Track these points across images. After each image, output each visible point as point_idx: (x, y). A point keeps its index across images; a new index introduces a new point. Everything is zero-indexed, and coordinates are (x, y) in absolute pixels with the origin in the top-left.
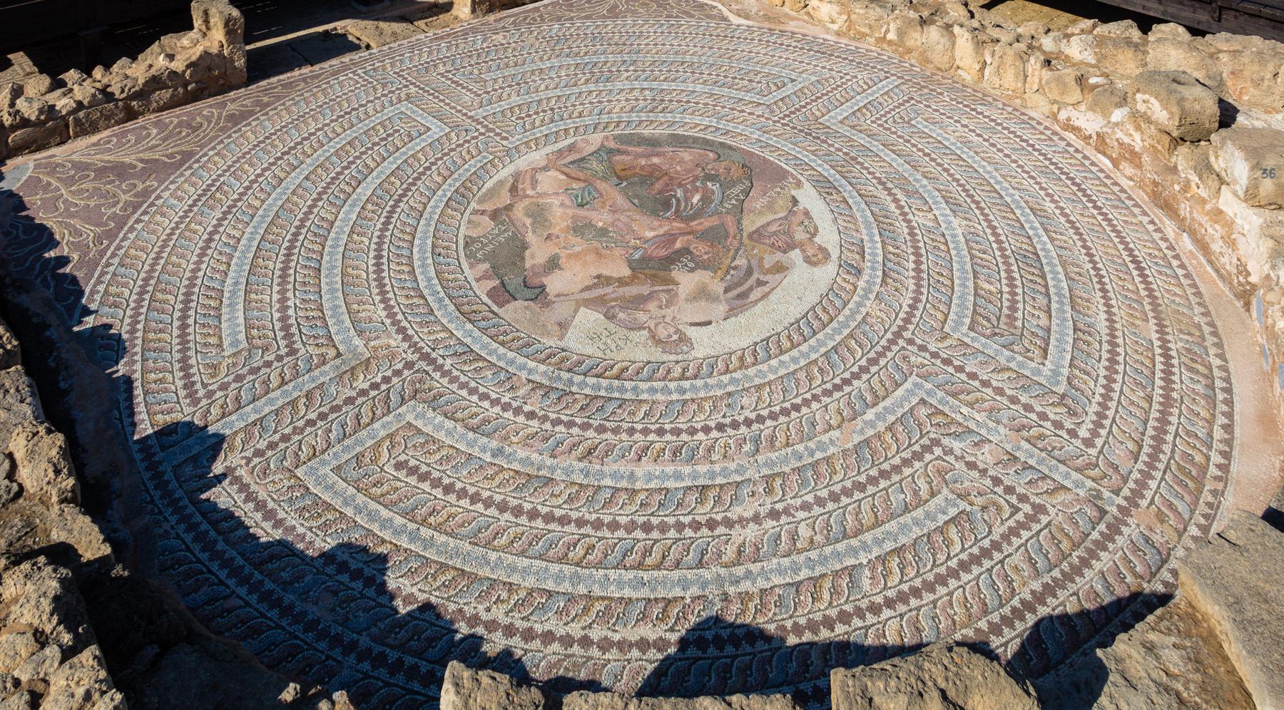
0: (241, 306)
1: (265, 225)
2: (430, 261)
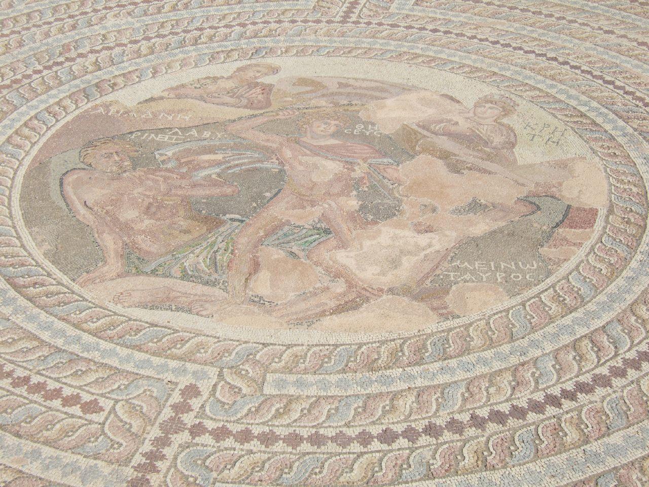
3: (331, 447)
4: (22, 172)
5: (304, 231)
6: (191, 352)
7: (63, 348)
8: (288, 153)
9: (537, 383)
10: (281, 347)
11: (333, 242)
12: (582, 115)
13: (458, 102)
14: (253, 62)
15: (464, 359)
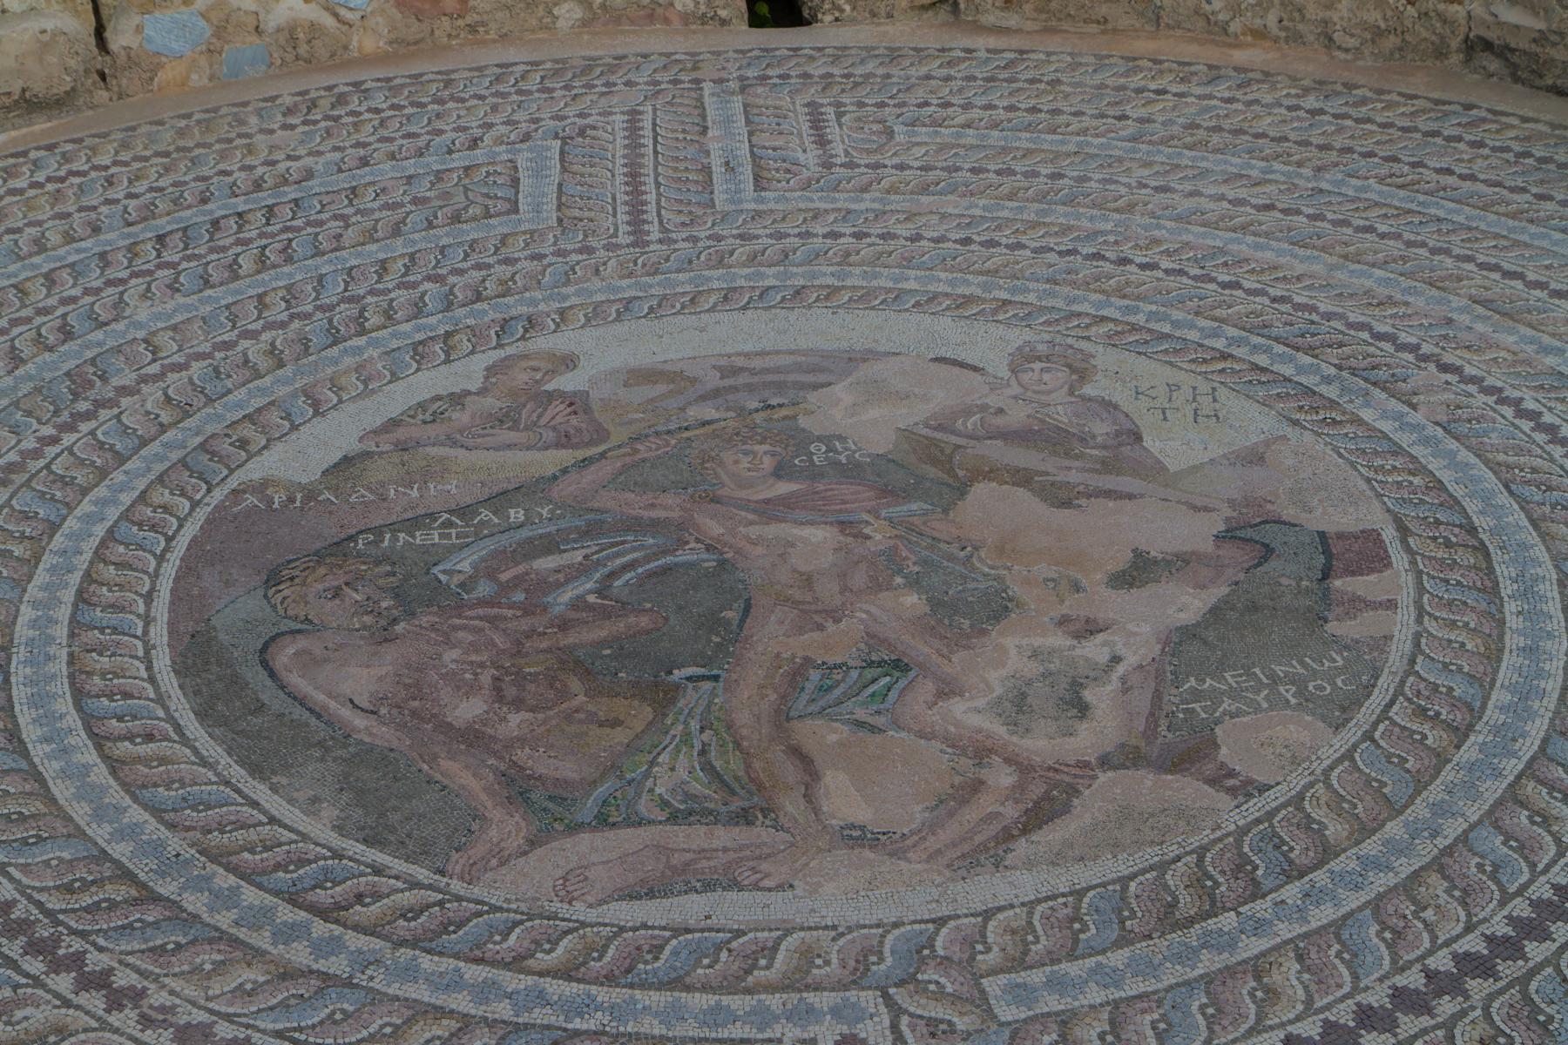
2: (1499, 696)
4: (162, 659)
5: (854, 674)
6: (798, 969)
7: (520, 1020)
8: (715, 528)
9: (1498, 883)
10: (973, 920)
11: (927, 688)
12: (1225, 357)
13: (975, 369)
14: (509, 350)
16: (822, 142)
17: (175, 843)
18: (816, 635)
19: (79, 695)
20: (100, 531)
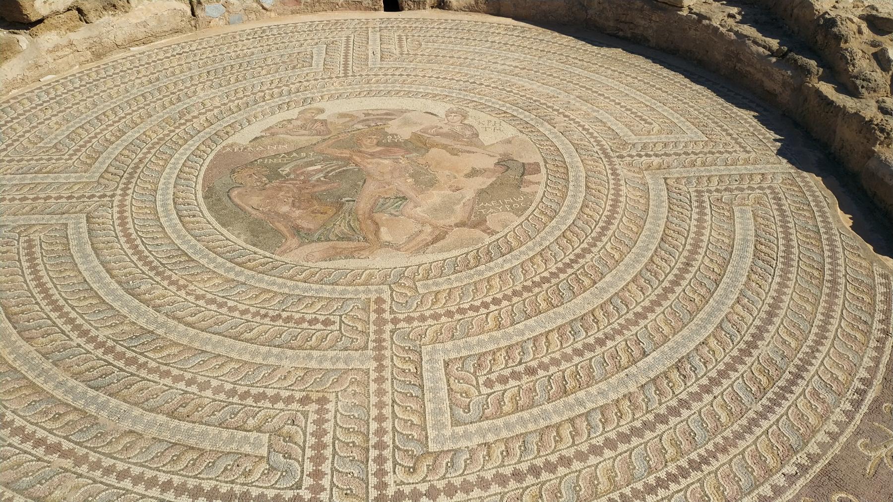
0: (738, 237)
1: (707, 308)
3: (471, 313)
4: (200, 195)
8: (358, 159)
11: (411, 205)
15: (513, 253)
16: (401, 47)
17: (200, 245)
18: (384, 189)
19: (175, 203)
20: (185, 158)
